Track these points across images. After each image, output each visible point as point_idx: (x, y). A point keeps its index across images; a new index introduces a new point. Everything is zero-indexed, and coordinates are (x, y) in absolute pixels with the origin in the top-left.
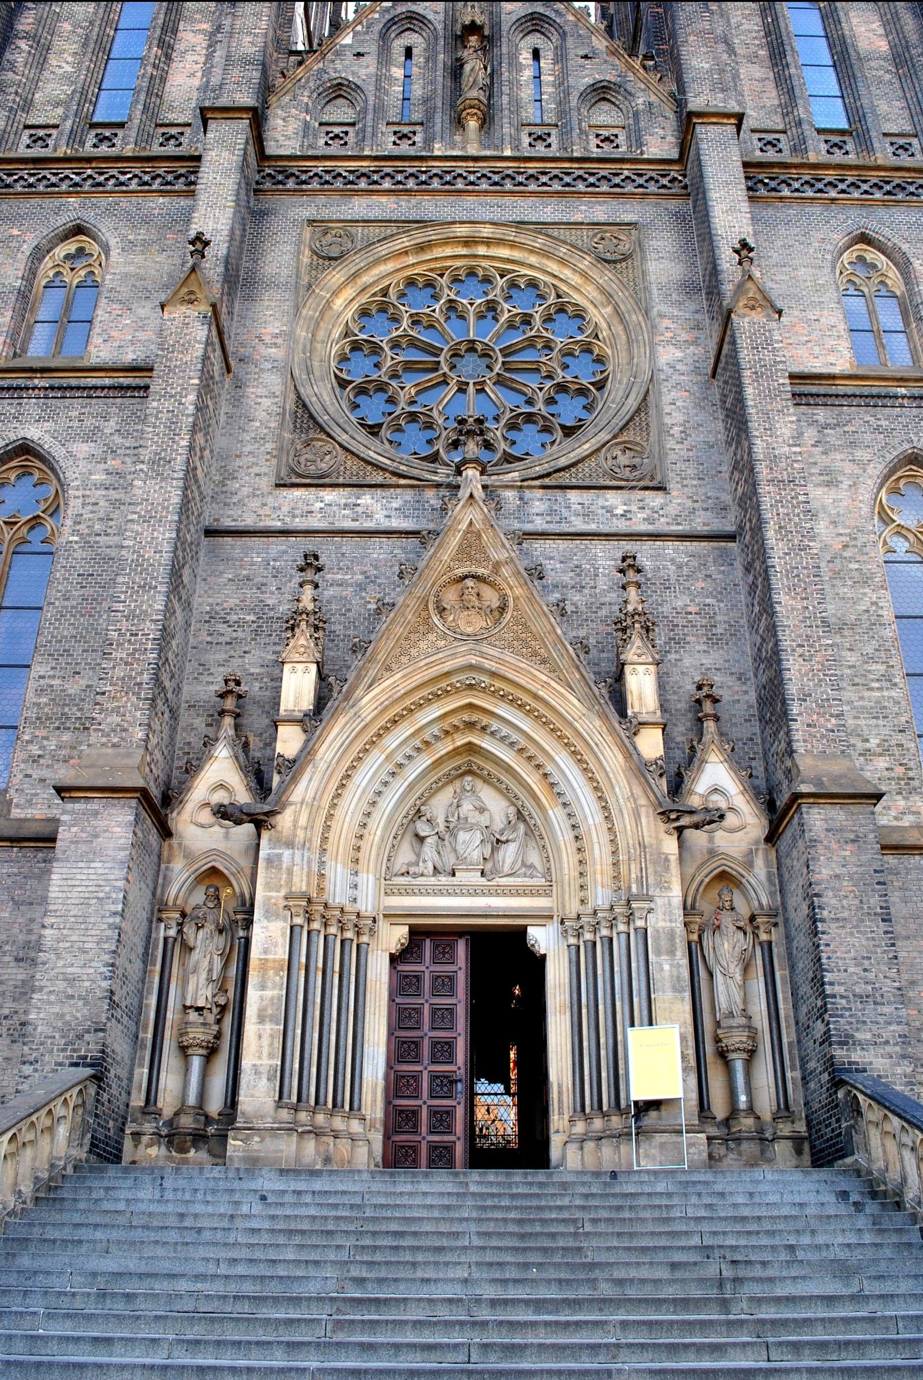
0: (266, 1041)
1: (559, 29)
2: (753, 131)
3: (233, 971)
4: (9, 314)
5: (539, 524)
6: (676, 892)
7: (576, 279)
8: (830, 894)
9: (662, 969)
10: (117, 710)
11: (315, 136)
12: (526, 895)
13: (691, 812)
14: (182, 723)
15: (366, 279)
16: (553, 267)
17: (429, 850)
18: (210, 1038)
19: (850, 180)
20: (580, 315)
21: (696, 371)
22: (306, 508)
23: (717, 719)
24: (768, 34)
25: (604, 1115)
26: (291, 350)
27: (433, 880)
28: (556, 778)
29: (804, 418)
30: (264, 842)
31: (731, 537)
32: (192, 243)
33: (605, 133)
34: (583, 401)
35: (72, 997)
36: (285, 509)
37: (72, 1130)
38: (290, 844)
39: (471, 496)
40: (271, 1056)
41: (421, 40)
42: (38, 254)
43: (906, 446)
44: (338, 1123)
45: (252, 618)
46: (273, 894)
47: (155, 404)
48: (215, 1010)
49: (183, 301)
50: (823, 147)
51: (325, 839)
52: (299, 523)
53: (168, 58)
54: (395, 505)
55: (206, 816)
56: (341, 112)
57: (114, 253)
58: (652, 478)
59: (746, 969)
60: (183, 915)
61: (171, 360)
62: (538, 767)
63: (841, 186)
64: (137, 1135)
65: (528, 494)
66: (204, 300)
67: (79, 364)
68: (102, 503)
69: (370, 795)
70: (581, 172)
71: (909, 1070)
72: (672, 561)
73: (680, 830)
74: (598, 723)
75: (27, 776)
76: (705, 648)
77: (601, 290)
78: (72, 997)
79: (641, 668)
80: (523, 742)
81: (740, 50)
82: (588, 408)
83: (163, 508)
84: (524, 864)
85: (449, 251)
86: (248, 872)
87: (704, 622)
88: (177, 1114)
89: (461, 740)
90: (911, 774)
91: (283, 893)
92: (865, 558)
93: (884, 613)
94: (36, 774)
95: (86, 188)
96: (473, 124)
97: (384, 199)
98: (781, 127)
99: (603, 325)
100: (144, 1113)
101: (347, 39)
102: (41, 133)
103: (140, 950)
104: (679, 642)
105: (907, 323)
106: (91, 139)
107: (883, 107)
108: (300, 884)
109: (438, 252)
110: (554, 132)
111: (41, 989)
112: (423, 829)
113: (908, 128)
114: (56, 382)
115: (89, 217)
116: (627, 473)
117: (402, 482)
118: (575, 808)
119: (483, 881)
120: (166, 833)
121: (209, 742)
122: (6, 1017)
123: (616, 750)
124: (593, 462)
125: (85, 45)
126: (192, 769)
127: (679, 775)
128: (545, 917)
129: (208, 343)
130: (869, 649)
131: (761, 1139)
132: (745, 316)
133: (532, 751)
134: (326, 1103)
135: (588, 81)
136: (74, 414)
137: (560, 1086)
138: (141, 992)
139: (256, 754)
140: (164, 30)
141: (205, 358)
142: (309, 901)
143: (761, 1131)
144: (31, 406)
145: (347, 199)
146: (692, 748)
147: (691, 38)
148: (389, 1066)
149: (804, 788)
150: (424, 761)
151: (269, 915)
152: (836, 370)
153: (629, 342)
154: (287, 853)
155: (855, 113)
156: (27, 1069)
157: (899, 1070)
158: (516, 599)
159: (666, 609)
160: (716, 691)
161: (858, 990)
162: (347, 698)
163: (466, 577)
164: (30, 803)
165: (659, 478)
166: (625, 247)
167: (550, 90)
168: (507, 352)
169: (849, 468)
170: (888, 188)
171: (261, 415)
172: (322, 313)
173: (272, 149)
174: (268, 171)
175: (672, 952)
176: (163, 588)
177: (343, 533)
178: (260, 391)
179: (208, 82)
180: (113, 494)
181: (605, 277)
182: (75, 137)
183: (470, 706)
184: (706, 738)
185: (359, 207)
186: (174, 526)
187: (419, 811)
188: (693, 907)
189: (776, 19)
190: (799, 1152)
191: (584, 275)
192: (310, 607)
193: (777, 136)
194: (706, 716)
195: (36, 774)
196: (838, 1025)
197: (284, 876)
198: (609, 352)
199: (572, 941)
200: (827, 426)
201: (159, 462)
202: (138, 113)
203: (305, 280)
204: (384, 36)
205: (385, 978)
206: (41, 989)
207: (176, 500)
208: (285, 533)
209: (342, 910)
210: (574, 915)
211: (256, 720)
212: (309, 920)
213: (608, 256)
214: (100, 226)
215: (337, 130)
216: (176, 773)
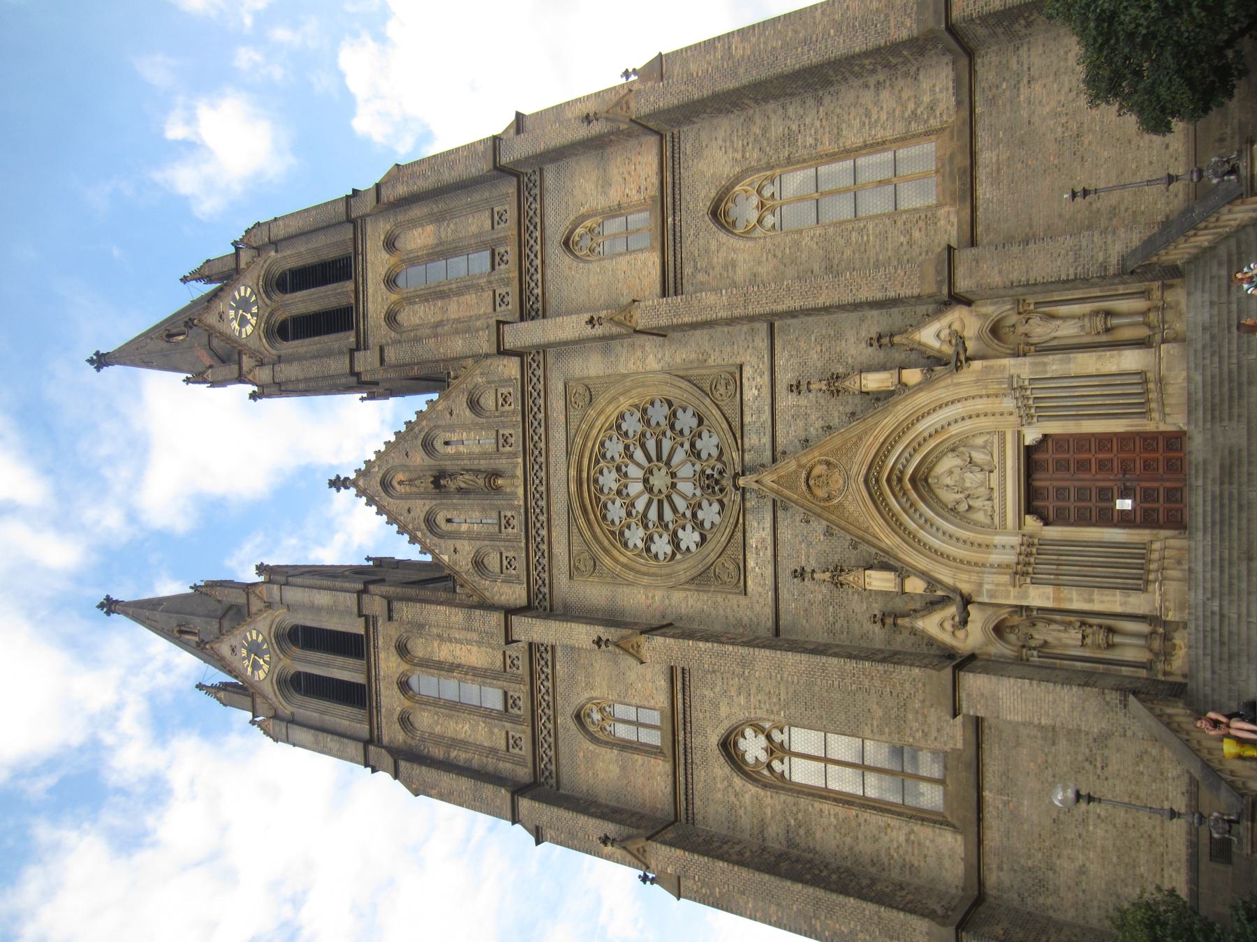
0: (1105, 598)
1: (431, 430)
2: (495, 310)
3: (1058, 617)
4: (636, 756)
5: (766, 440)
6: (1006, 361)
7: (602, 419)
8: (1011, 276)
9: (1056, 370)
10: (902, 685)
11: (511, 576)
12: (1005, 446)
13: (958, 354)
14: (899, 648)
15: (606, 543)
16: (595, 432)
17: (976, 503)
18: (1102, 631)
19: (527, 251)
20: (622, 416)
21: (662, 346)
22: (759, 577)
23: (892, 336)
24: (427, 300)
25: (1148, 401)
26: (656, 587)
27: (996, 501)
28: (932, 430)
29: (690, 281)
30: (980, 600)
31: (772, 326)
32: (600, 647)
33: (500, 401)
34: (680, 413)
35: (1083, 708)
36: (760, 590)
37: (1167, 706)
38: (980, 585)
39: (757, 482)
40: (1114, 595)
41: (441, 514)
42: (595, 740)
43: (707, 218)
44: (1155, 556)
45: (831, 609)
46: (1012, 594)
47: (706, 666)
48: (1084, 628)
49: (637, 651)
50: (503, 266)
51: (976, 564)
52: (770, 581)
53: (459, 666)
54: (756, 525)
55: (961, 634)
56: (493, 561)
57: (594, 694)
58: (732, 374)
59: (1052, 317)
60: (1023, 646)
61: (677, 658)
62: (925, 440)
63: (532, 256)
64: (1165, 673)
65: (746, 446)
66: (638, 639)
67: (669, 714)
68: (759, 697)
69: (946, 538)
70: (531, 416)
71: (1123, 230)
72: (787, 361)
73: (968, 359)
74: (899, 407)
75: (936, 739)
76: (844, 341)
77: (609, 403)
78: (1083, 708)
79: (864, 382)
80: (910, 449)
81: (438, 318)
83: (773, 659)
84: (984, 447)
85: (586, 495)
86: (995, 609)
87: (827, 342)
88: (1151, 650)
89: (909, 486)
90: (923, 217)
91: (1011, 589)
92: (782, 244)
93: (818, 233)
94: (934, 734)
95: (551, 712)
97: (554, 534)
98: (491, 293)
99: (631, 401)
100: (1151, 669)
101: (446, 558)
102: (511, 741)
103: (1048, 671)
104: (840, 356)
105: (621, 215)
106: (515, 711)
107: (473, 229)
108: (1006, 579)
109: (587, 502)
110: (501, 432)
111: (1078, 725)
112: (963, 507)
113: (488, 213)
114: (681, 727)
115: (570, 710)
116: (731, 387)
117: (741, 521)
118: (951, 419)
119: (996, 471)
120: (972, 657)
121: (914, 632)
122: (1091, 751)
123: (916, 397)
124: (725, 409)
125: (451, 717)
126: (931, 642)
127: (929, 358)
128: (1020, 436)
129: (664, 635)
130: (842, 242)
131: (1163, 308)
132: (637, 322)
133: (915, 444)
134: (1142, 564)
135: (468, 412)
136: (701, 716)
137: (1128, 426)
138: (1074, 671)
139: (918, 606)
140: (442, 669)
141: (673, 636)
142: (1016, 573)
143: (1157, 308)
144: (697, 741)
145: (554, 557)
146: (911, 350)
147: (441, 350)
148: (1116, 526)
149: (945, 291)
150: (922, 506)
151: (1025, 596)
152: (658, 261)
153: (643, 386)
154: (986, 587)
155: (480, 247)
156: (1129, 733)
157: (1123, 236)
158: (821, 455)
159: (819, 364)
160: (875, 336)
161: (1072, 260)
162: (887, 553)
163: (808, 484)
164: (953, 737)
165: (733, 369)
166: (581, 390)
167: (472, 434)
168: (649, 459)
169: (722, 254)
170: (532, 228)
171: (699, 604)
172: (631, 569)
173: (523, 601)
174: (536, 604)
175: (1045, 364)
176: (824, 659)
177: (775, 556)
178: (683, 606)
179: (476, 642)
180: (753, 691)
181: (601, 402)
182: (515, 720)
183: (889, 480)
184: (904, 341)
185: (560, 549)
186: (784, 653)
187: (951, 509)
188: (1014, 349)
189: (418, 296)
190: (1171, 286)
191: (599, 414)
192: (828, 574)
193: (497, 296)
194: (890, 342)
195: (934, 734)
196: (1094, 270)
197: (1001, 588)
198: (648, 398)
199: (1035, 419)
200: (695, 267)
201: (743, 663)
202: (499, 683)
203: (609, 580)
204: (441, 536)
205: (1060, 529)
206: (1078, 725)
207: (768, 652)
209: (1020, 554)
210: (1019, 420)
211: (899, 604)
212: (1028, 573)
213: (587, 399)
214: (576, 703)
215: (505, 563)
216: (932, 652)
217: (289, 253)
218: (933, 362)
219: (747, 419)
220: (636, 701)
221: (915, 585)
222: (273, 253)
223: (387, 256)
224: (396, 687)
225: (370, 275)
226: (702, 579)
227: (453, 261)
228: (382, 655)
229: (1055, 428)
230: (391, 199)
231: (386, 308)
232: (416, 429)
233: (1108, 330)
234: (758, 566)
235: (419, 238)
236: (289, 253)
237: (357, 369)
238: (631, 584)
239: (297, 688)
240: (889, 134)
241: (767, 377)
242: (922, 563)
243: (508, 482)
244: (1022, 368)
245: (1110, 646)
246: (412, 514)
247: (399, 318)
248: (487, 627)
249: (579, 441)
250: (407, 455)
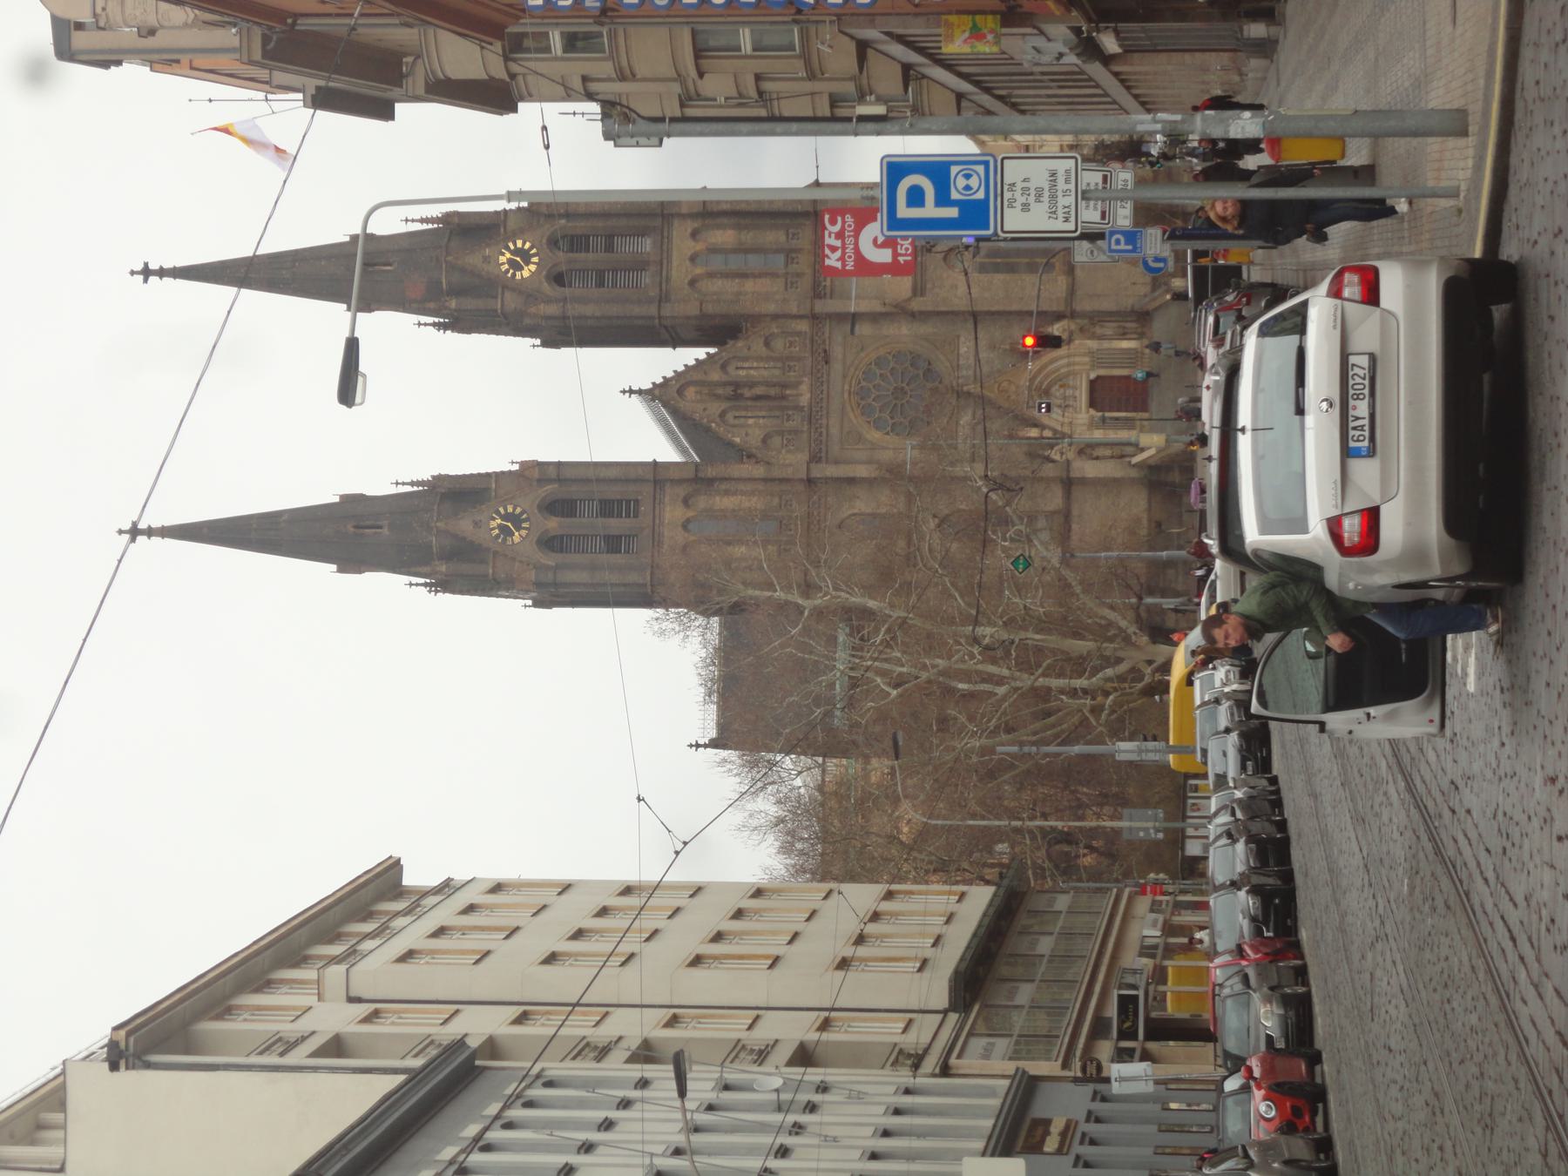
5: (971, 373)
17: (1071, 403)
56: (776, 441)
57: (856, 511)
59: (1102, 327)
82: (919, 356)
96: (788, 392)
108: (1085, 428)
128: (1088, 376)
135: (764, 349)
147: (756, 309)
155: (777, 251)
185: (834, 431)
204: (734, 426)
217: (582, 224)
219: (961, 362)
221: (1047, 433)
222: (563, 222)
223: (693, 244)
224: (680, 529)
225: (675, 254)
227: (750, 257)
228: (668, 509)
229: (1103, 372)
230: (715, 210)
231: (690, 277)
232: (716, 358)
233: (1124, 334)
235: (724, 237)
236: (582, 224)
237: (662, 313)
239: (553, 551)
241: (973, 343)
243: (794, 392)
244: (1092, 344)
246: (707, 412)
247: (697, 285)
248: (784, 475)
249: (852, 370)
250: (705, 373)
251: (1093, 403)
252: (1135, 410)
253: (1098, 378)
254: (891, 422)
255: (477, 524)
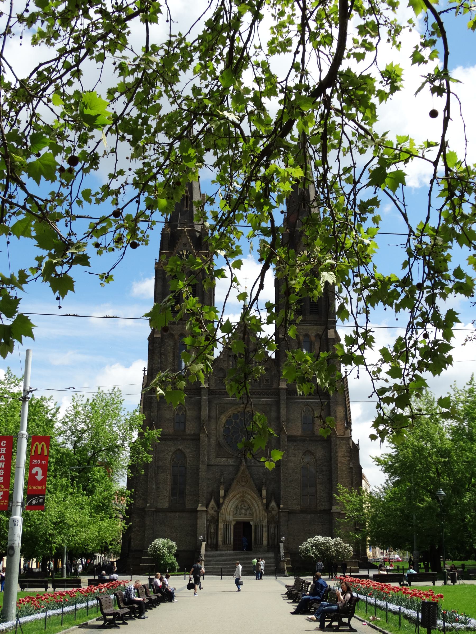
108: (224, 519)
125: (174, 354)
128: (252, 520)
208: (218, 466)
218: (268, 505)
220: (187, 424)
225: (309, 327)
226: (219, 445)
229: (253, 528)
234: (223, 461)
238: (217, 423)
240: (318, 495)
242: (226, 502)
244: (265, 523)
245: (211, 538)
251: (238, 523)
252: (235, 544)
253: (251, 526)
254: (230, 427)
255: (185, 245)
